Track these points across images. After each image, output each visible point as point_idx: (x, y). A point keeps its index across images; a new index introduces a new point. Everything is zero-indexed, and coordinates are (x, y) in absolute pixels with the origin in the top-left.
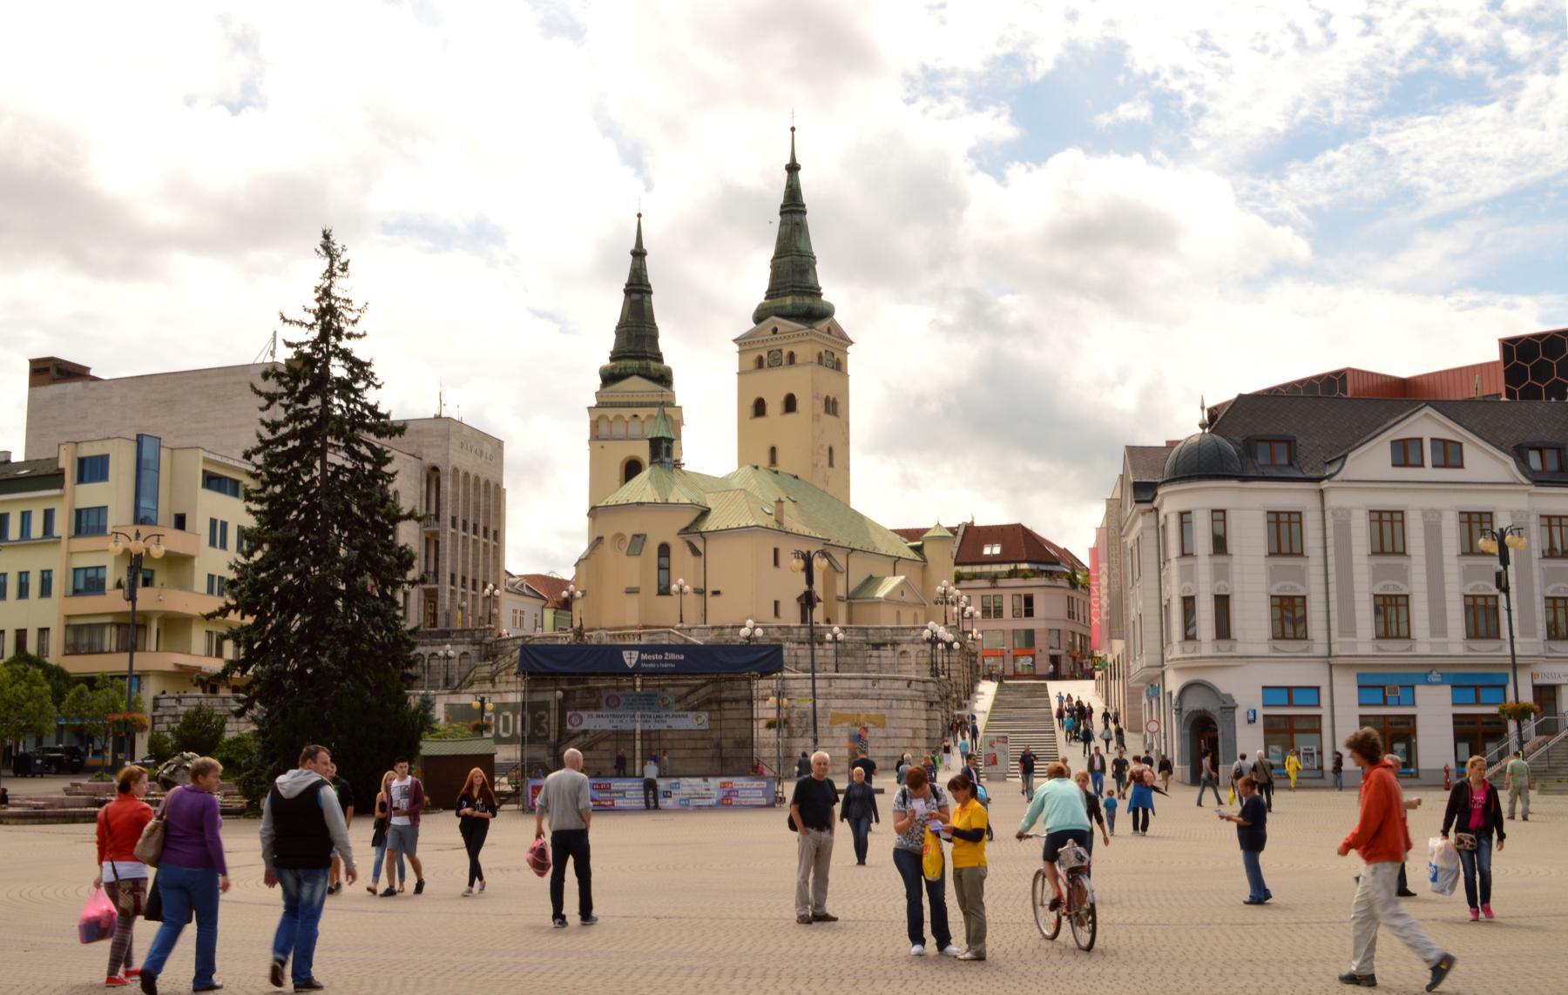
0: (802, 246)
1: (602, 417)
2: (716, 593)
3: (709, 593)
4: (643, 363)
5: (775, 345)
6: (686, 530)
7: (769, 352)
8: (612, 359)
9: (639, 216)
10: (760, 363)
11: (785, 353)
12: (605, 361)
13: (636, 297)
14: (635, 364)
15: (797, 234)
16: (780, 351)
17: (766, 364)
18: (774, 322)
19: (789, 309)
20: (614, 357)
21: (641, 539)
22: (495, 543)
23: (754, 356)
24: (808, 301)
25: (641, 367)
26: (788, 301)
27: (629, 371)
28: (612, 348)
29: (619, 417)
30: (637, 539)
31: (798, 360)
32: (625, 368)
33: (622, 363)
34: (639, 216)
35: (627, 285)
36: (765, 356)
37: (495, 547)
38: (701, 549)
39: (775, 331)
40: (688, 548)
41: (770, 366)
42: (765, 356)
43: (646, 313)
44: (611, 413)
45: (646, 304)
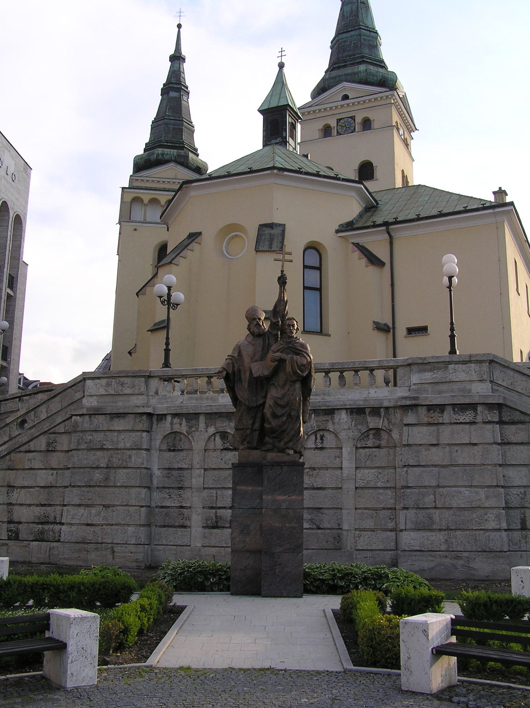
0: (369, 24)
1: (136, 200)
2: (411, 331)
3: (401, 331)
4: (182, 152)
5: (345, 113)
6: (349, 226)
7: (339, 120)
8: (145, 150)
9: (179, 26)
10: (327, 131)
11: (359, 119)
12: (140, 151)
13: (173, 94)
14: (174, 152)
15: (364, 11)
16: (353, 118)
17: (334, 132)
18: (345, 88)
19: (363, 76)
20: (149, 147)
21: (276, 231)
22: (9, 291)
23: (320, 125)
24: (381, 70)
25: (179, 155)
26: (362, 67)
27: (166, 157)
28: (147, 141)
29: (154, 201)
30: (268, 231)
31: (375, 125)
32: (163, 155)
33: (160, 150)
34: (179, 26)
35: (164, 85)
36: (333, 123)
37: (9, 297)
38: (385, 257)
39: (346, 97)
40: (357, 253)
41: (339, 134)
42: (333, 123)
43: (183, 109)
44: (146, 196)
45: (183, 102)
